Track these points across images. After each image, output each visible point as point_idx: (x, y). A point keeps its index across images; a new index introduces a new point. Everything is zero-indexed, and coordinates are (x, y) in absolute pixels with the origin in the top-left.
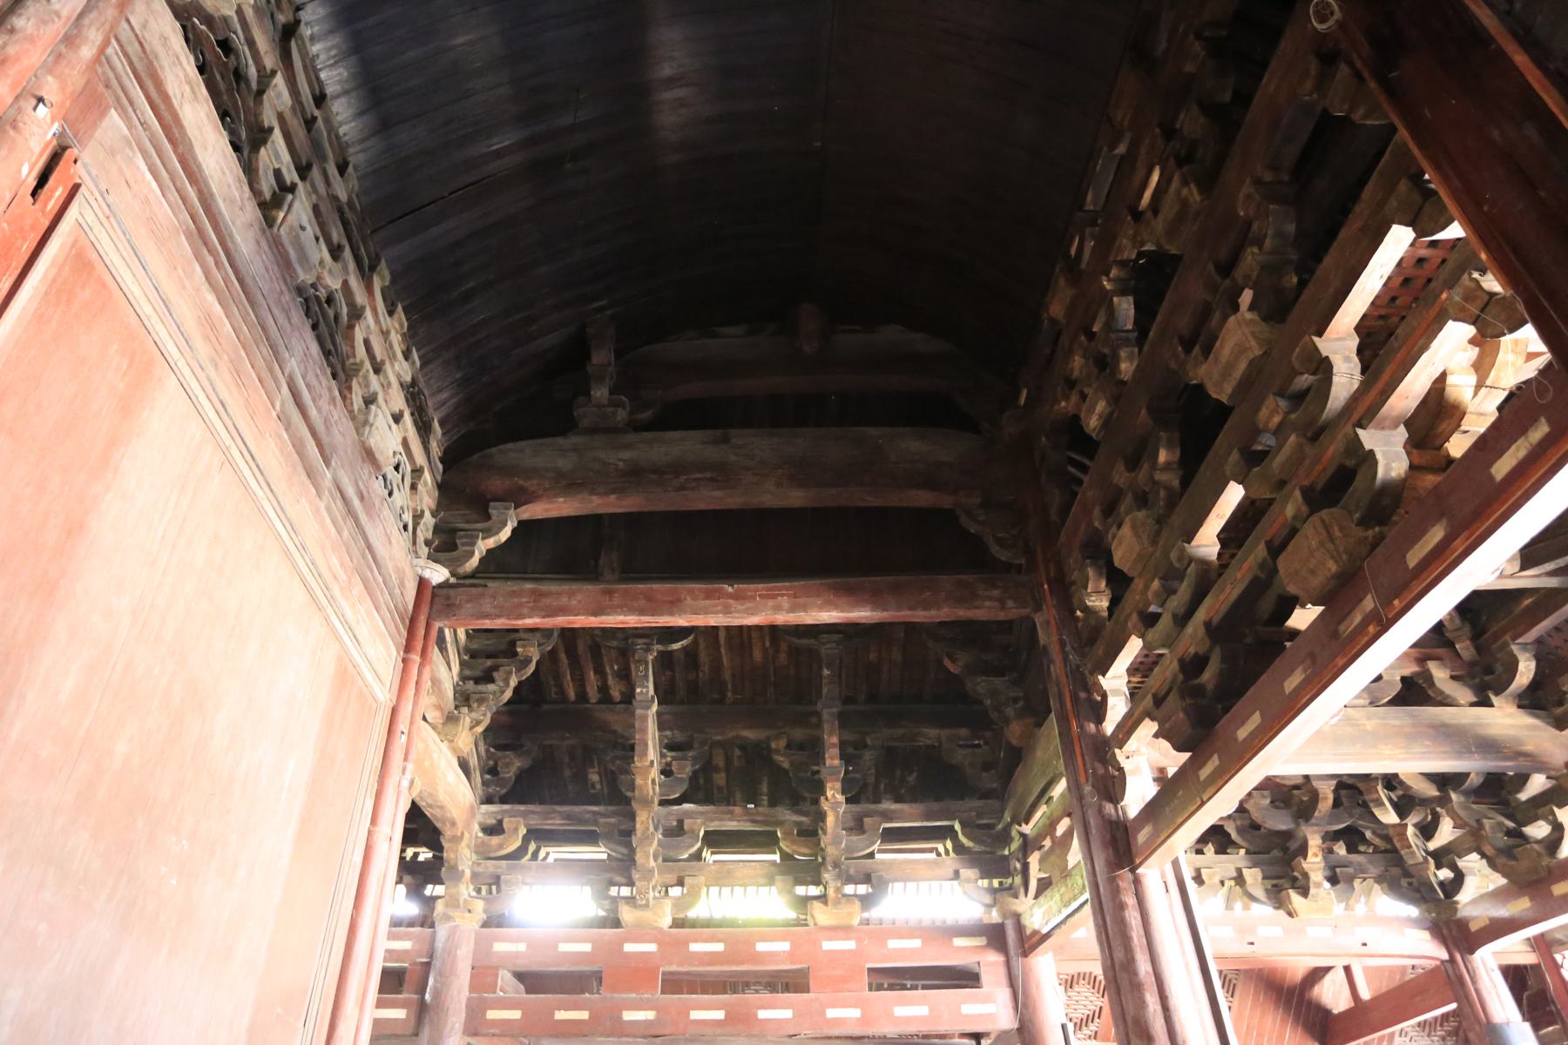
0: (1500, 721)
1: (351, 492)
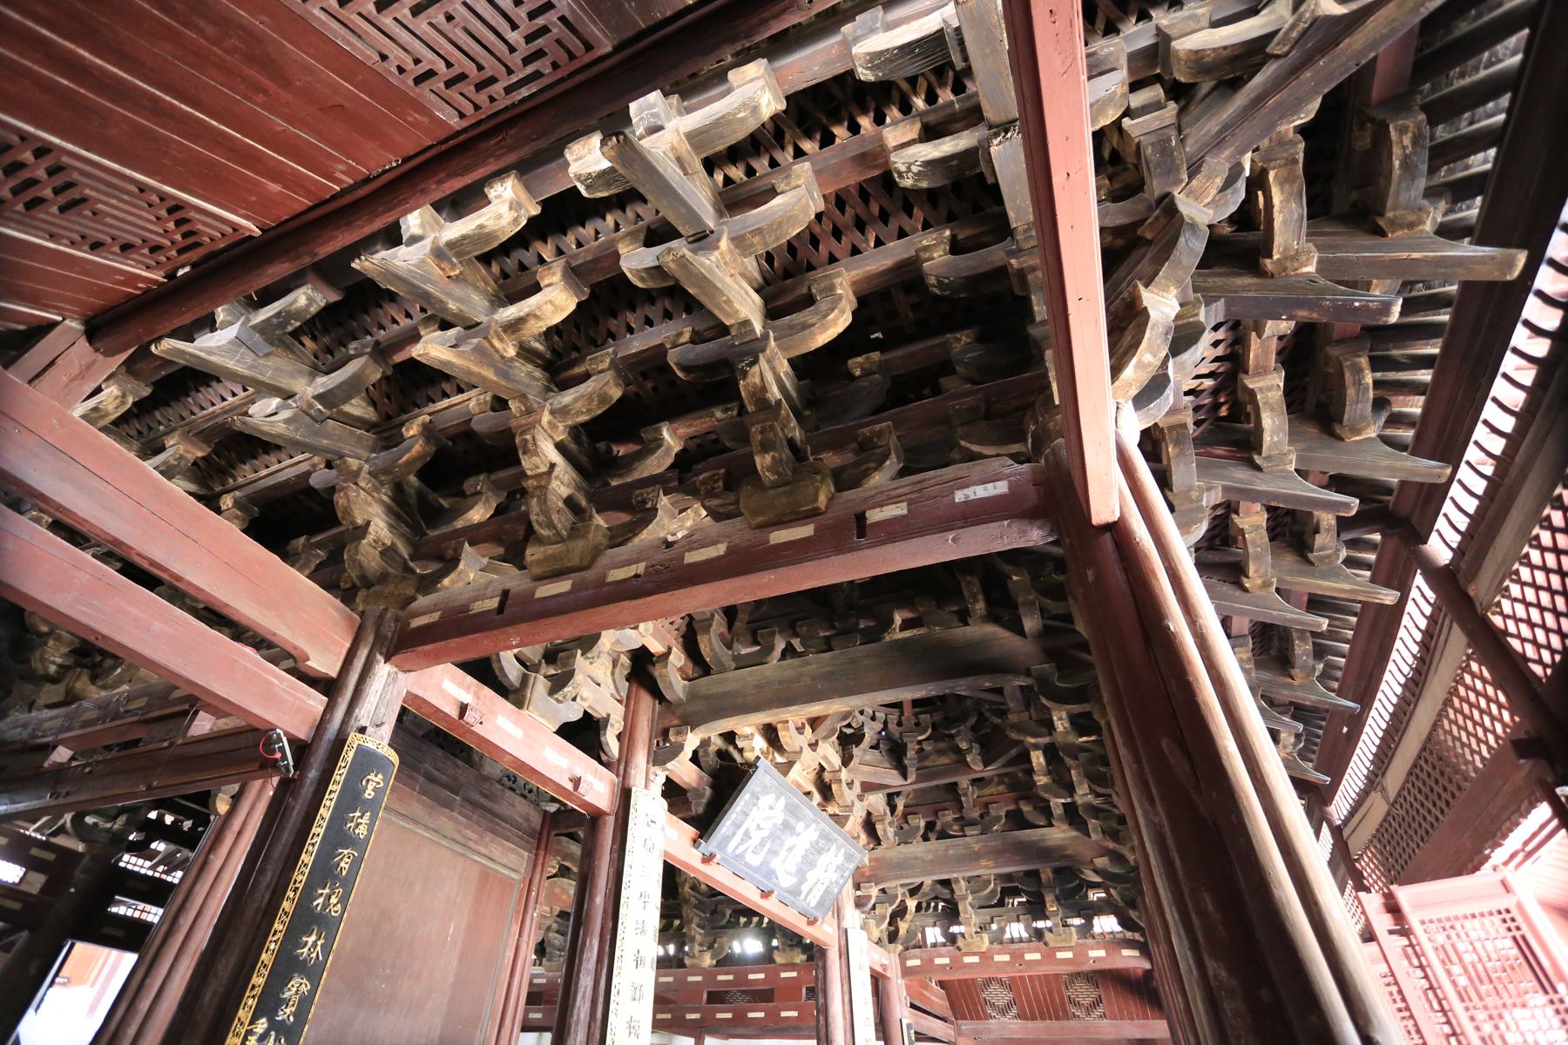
1: (477, 797)
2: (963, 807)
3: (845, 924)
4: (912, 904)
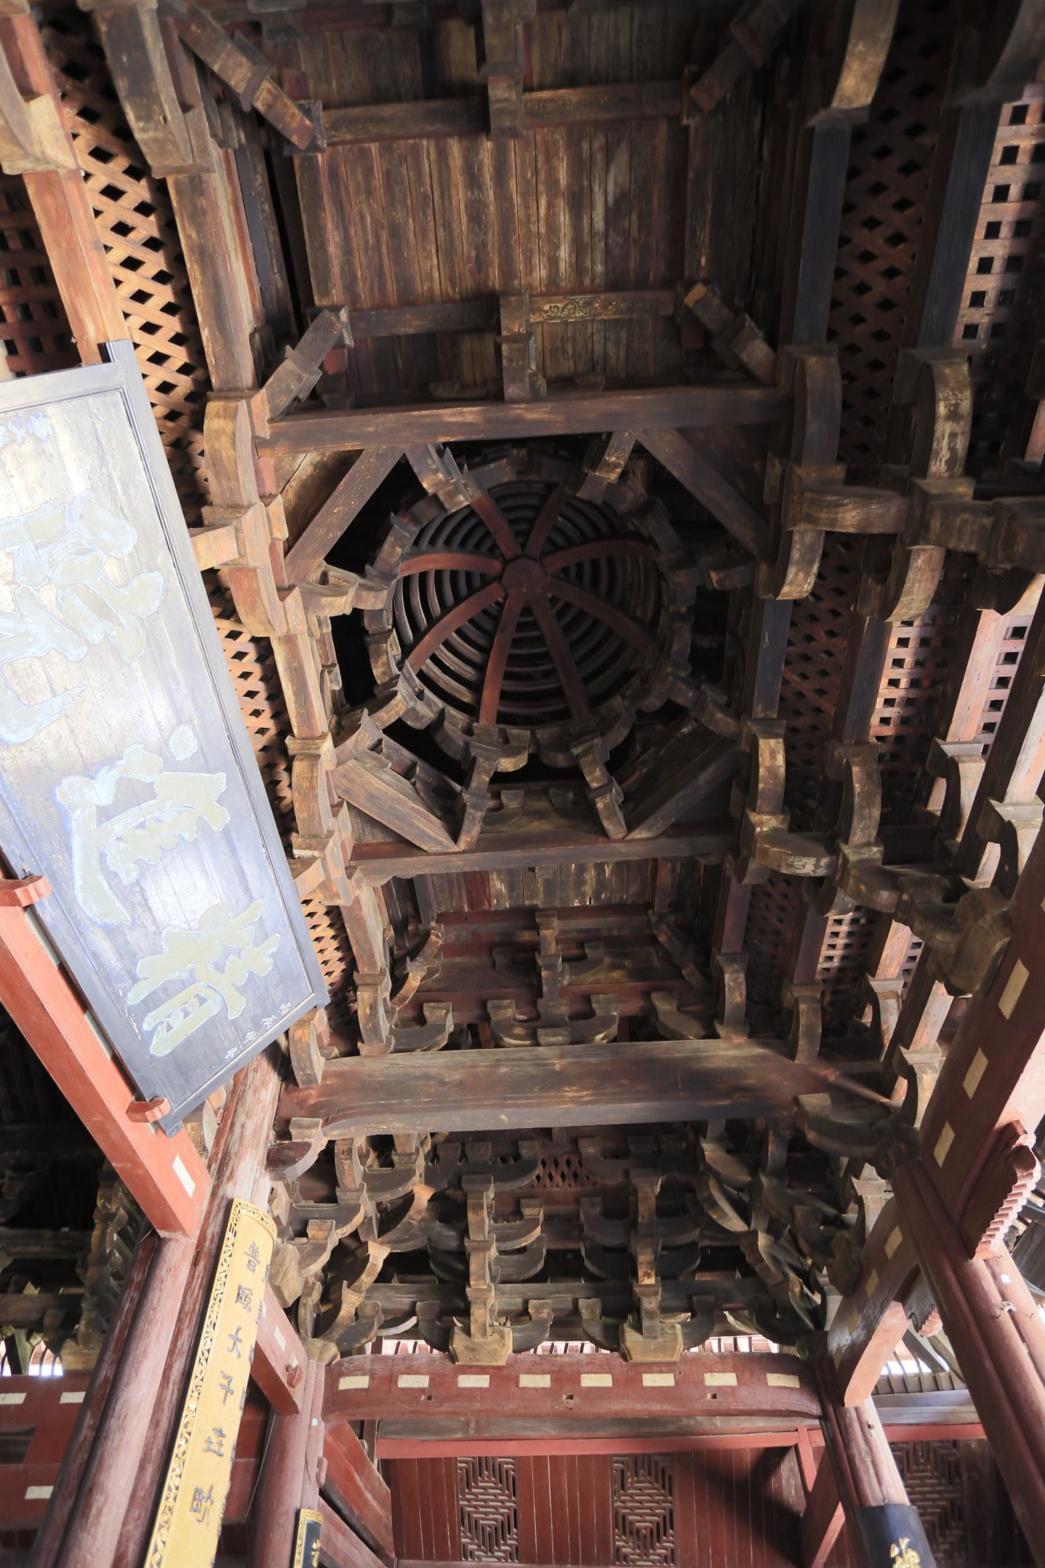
0: (722, 1053)
2: (540, 994)
3: (229, 1190)
4: (378, 1253)
